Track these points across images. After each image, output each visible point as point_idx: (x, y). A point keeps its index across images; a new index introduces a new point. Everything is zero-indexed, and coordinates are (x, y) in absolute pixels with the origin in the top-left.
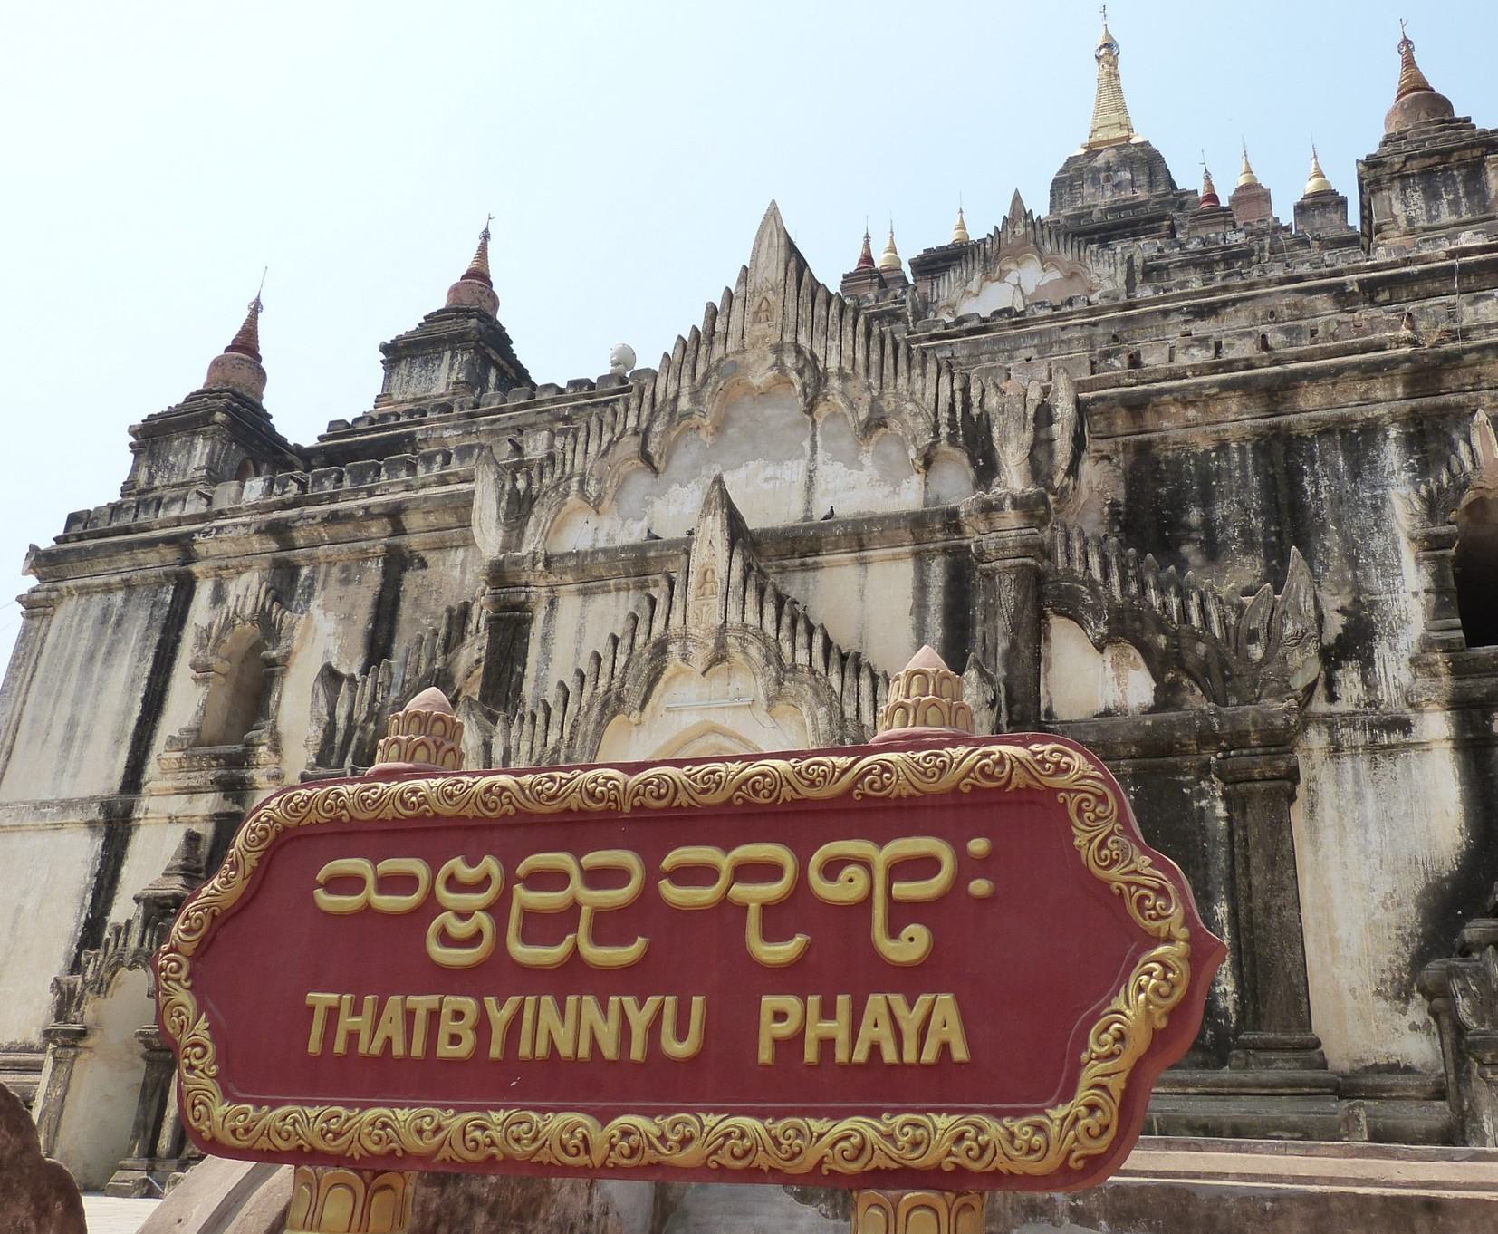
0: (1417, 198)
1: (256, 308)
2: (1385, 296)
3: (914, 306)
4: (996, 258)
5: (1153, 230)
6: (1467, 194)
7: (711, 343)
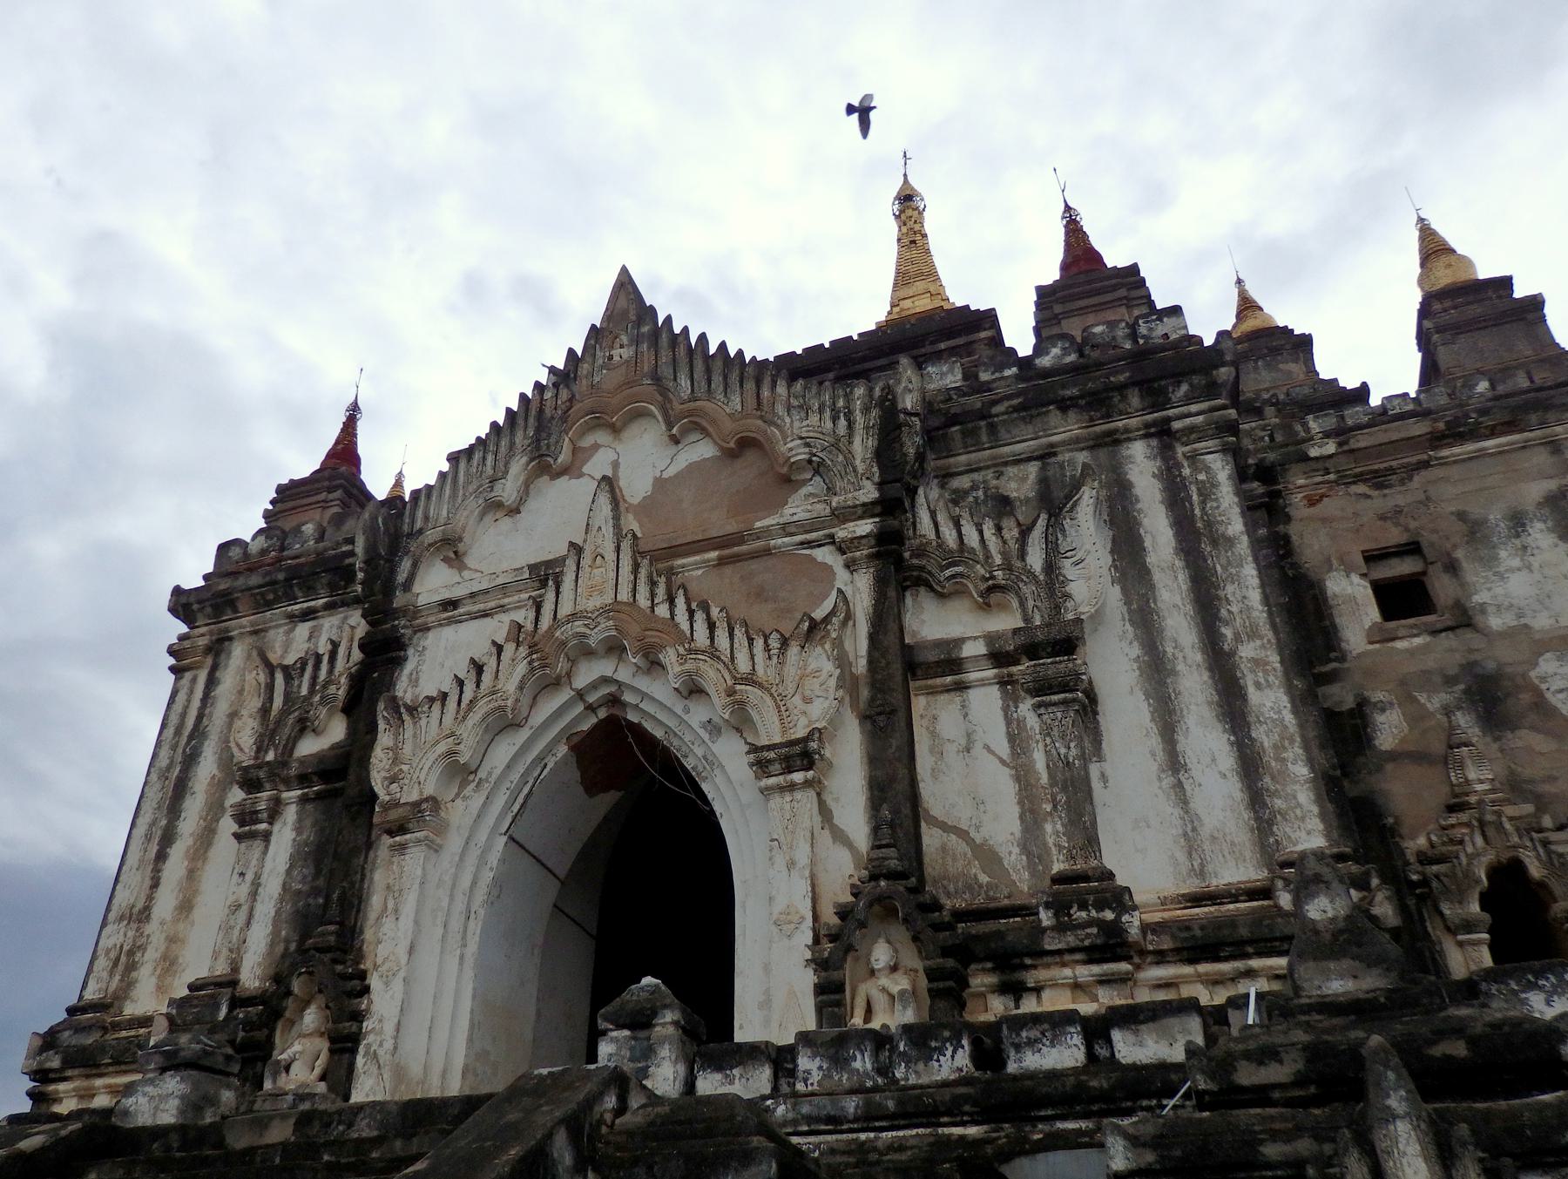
3: (371, 549)
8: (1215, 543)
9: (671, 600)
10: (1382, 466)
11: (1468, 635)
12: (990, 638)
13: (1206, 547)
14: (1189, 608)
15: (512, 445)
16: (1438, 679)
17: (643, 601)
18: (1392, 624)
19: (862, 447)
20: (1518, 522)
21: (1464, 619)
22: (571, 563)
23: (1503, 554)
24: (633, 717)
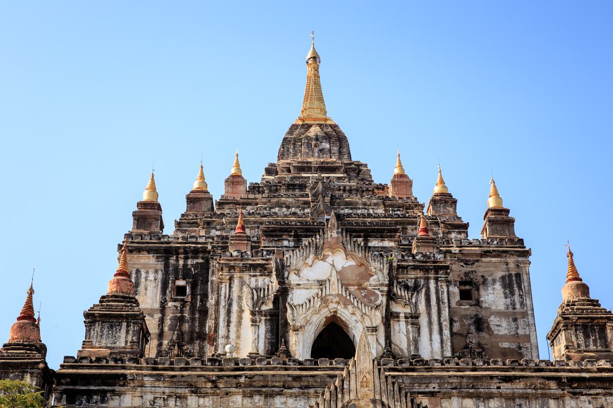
0: (581, 336)
1: (31, 292)
2: (576, 385)
4: (322, 248)
5: (391, 237)
6: (600, 338)
7: (343, 394)
8: (442, 303)
9: (350, 295)
10: (468, 259)
11: (478, 307)
12: (405, 313)
13: (441, 303)
14: (437, 314)
15: (310, 251)
16: (469, 317)
17: (344, 295)
18: (462, 301)
19: (386, 271)
20: (494, 281)
21: (478, 303)
22: (328, 283)
23: (489, 289)
24: (338, 315)
